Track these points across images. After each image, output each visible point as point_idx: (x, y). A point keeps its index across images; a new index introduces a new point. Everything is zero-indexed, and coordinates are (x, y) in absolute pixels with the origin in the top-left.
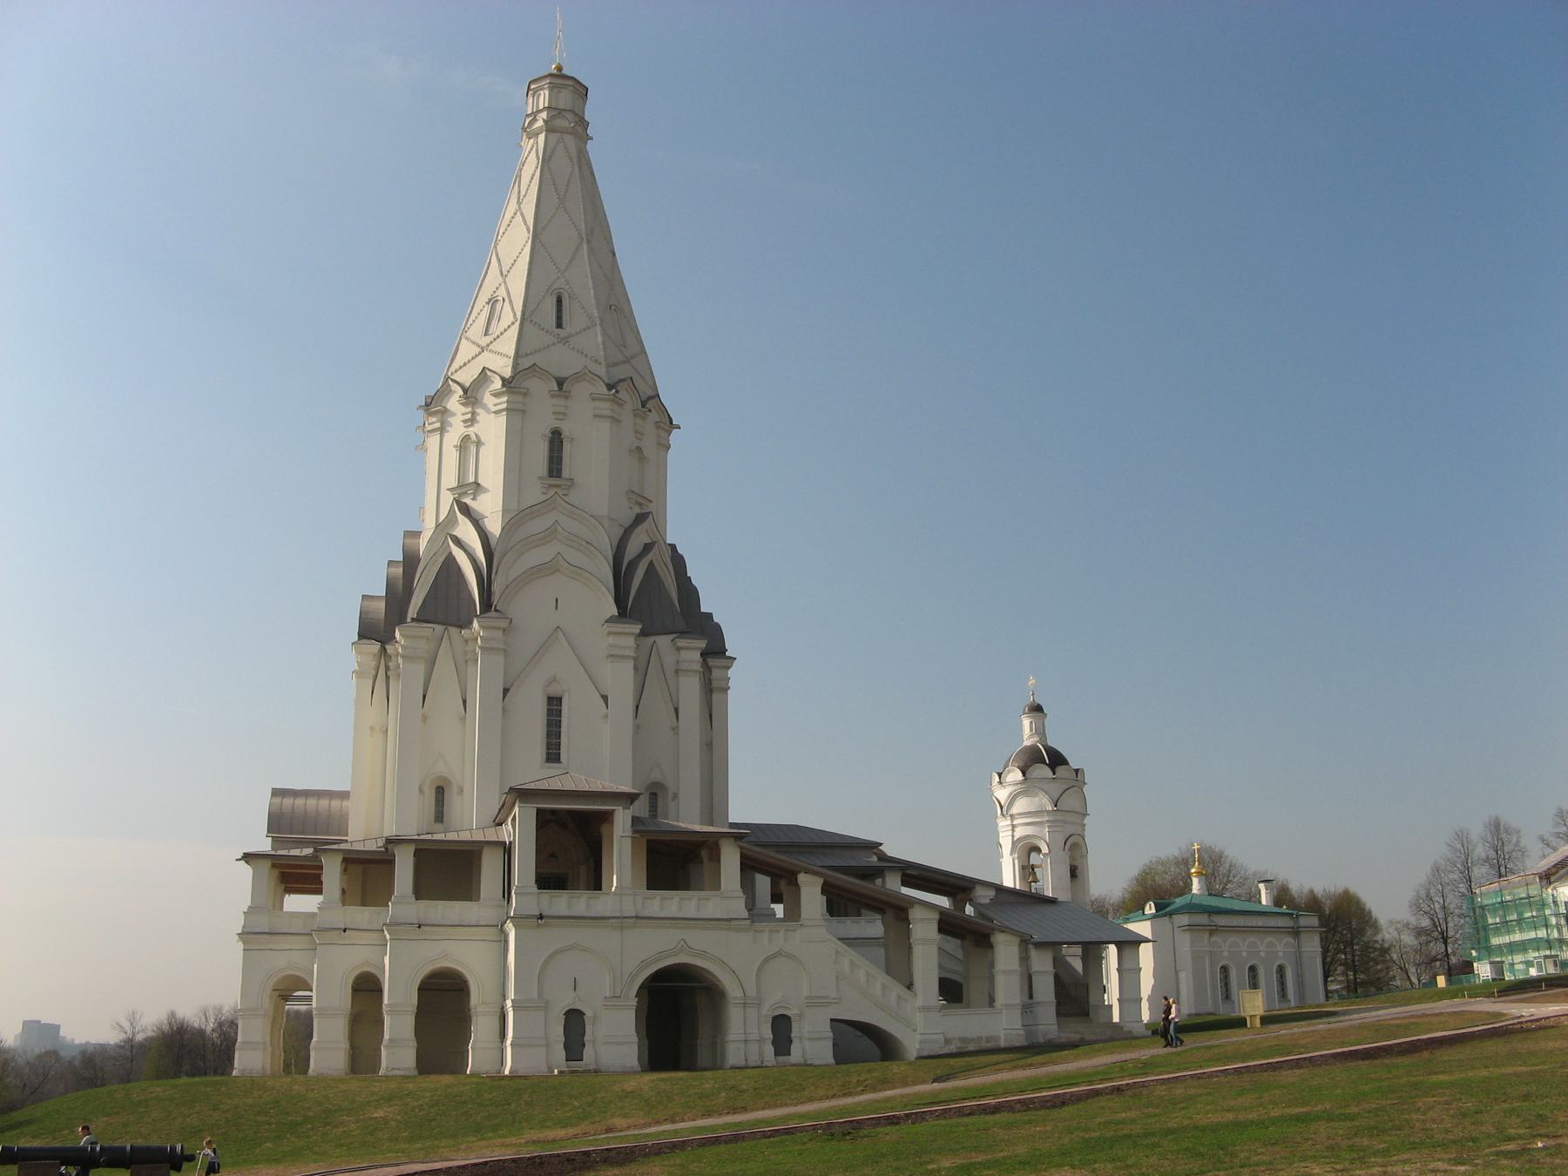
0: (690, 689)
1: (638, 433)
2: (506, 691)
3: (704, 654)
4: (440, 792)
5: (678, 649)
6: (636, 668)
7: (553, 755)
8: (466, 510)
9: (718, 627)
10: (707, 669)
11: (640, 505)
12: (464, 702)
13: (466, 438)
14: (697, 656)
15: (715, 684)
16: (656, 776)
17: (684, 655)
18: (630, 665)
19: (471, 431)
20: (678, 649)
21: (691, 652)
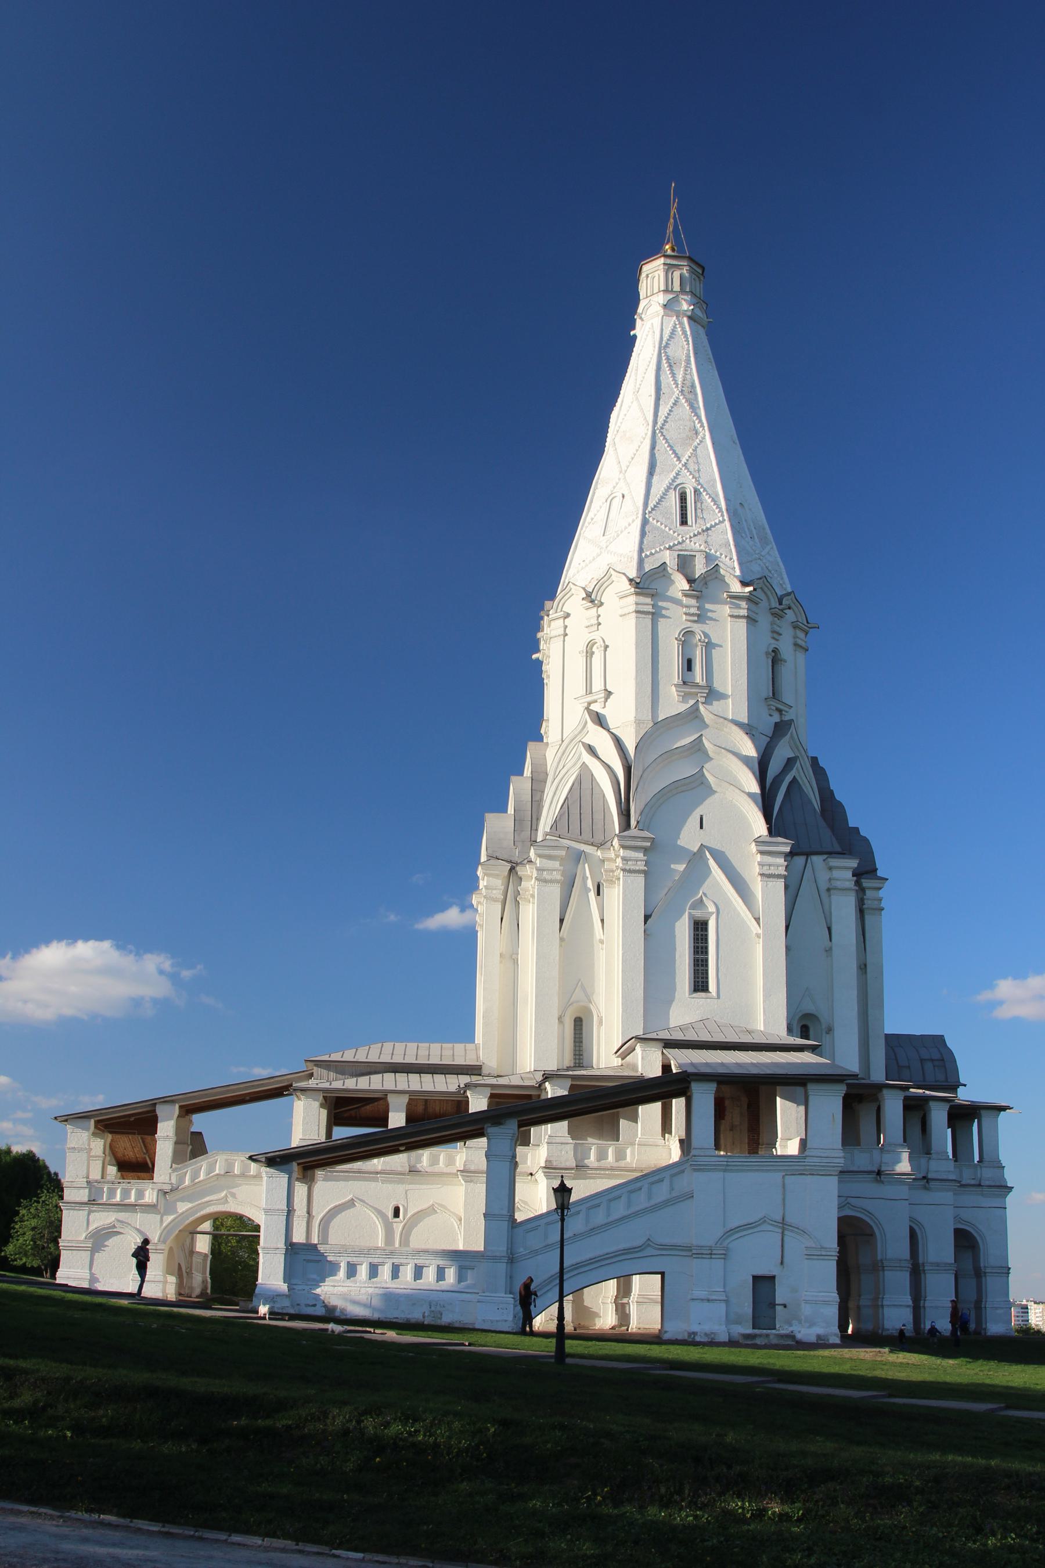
0: (844, 907)
1: (776, 634)
2: (647, 918)
3: (858, 874)
4: (578, 1023)
5: (830, 868)
6: (786, 887)
7: (700, 985)
8: (599, 720)
9: (866, 840)
10: (861, 890)
11: (780, 711)
12: (829, 929)
13: (591, 644)
14: (849, 874)
15: (868, 903)
16: (810, 1008)
17: (836, 874)
18: (780, 884)
19: (596, 636)
20: (830, 868)
21: (843, 870)
